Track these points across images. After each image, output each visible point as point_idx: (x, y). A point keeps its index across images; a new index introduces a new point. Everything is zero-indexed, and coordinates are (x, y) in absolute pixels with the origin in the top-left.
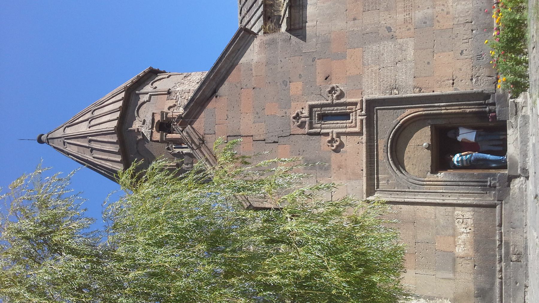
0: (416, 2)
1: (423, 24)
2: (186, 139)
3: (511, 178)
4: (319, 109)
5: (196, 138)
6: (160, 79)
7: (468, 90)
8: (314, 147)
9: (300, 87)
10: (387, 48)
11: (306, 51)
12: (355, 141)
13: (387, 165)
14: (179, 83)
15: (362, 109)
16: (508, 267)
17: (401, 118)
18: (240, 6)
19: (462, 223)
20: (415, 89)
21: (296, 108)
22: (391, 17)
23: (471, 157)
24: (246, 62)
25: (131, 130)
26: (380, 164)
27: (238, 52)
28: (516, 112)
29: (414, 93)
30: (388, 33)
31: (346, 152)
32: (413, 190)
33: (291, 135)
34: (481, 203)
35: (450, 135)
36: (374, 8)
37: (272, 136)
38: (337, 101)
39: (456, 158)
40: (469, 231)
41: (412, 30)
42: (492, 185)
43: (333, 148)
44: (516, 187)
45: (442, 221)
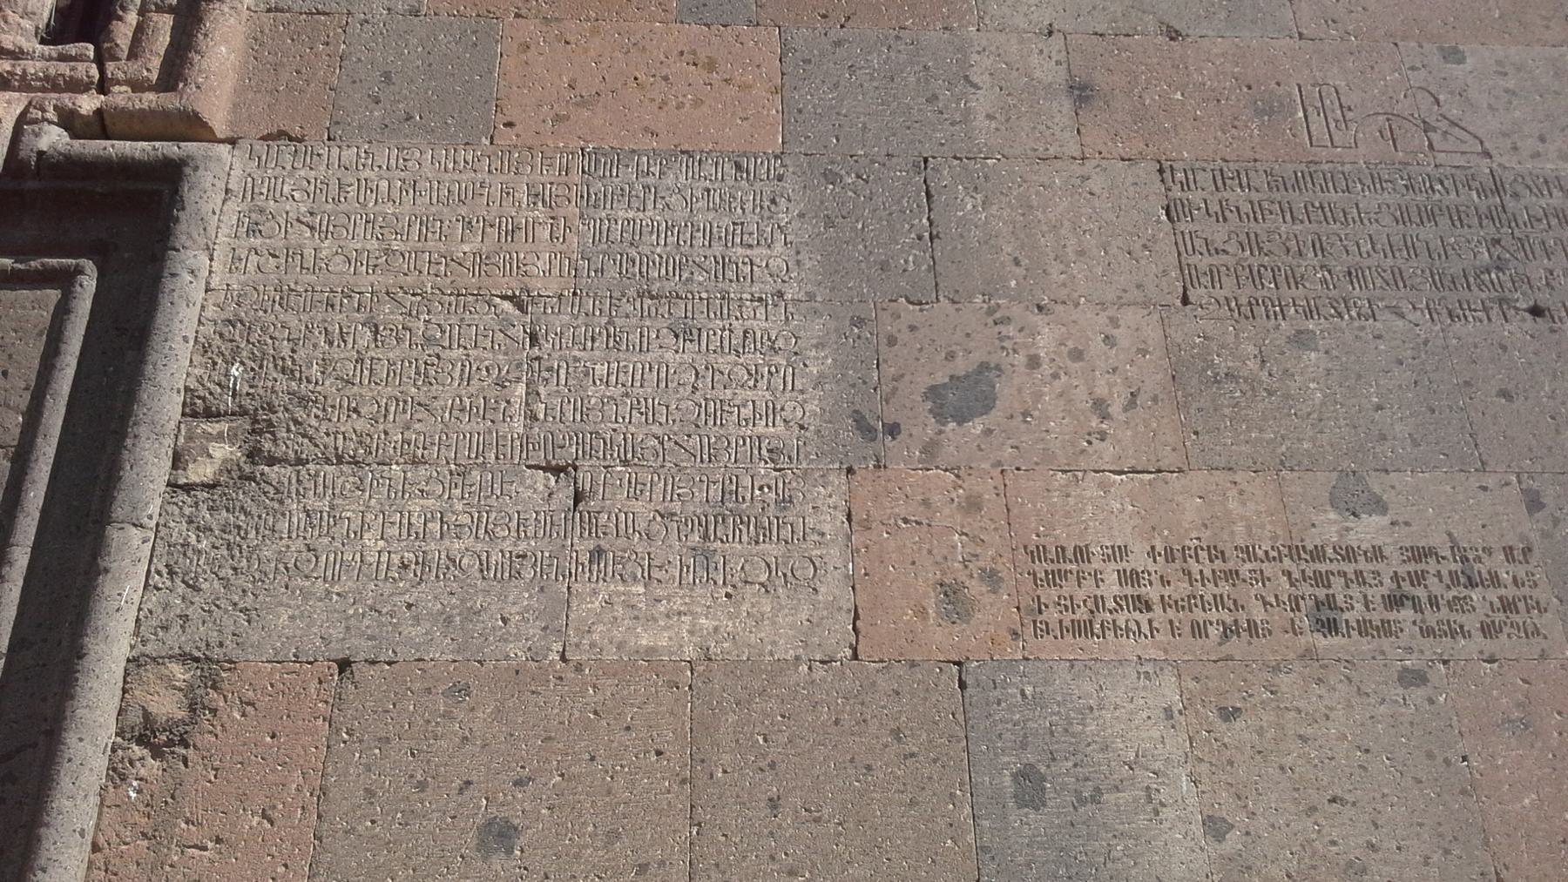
0: (1284, 680)
10: (755, 375)
20: (179, 672)
22: (1105, 417)
30: (924, 382)
36: (1203, 262)
41: (942, 638)
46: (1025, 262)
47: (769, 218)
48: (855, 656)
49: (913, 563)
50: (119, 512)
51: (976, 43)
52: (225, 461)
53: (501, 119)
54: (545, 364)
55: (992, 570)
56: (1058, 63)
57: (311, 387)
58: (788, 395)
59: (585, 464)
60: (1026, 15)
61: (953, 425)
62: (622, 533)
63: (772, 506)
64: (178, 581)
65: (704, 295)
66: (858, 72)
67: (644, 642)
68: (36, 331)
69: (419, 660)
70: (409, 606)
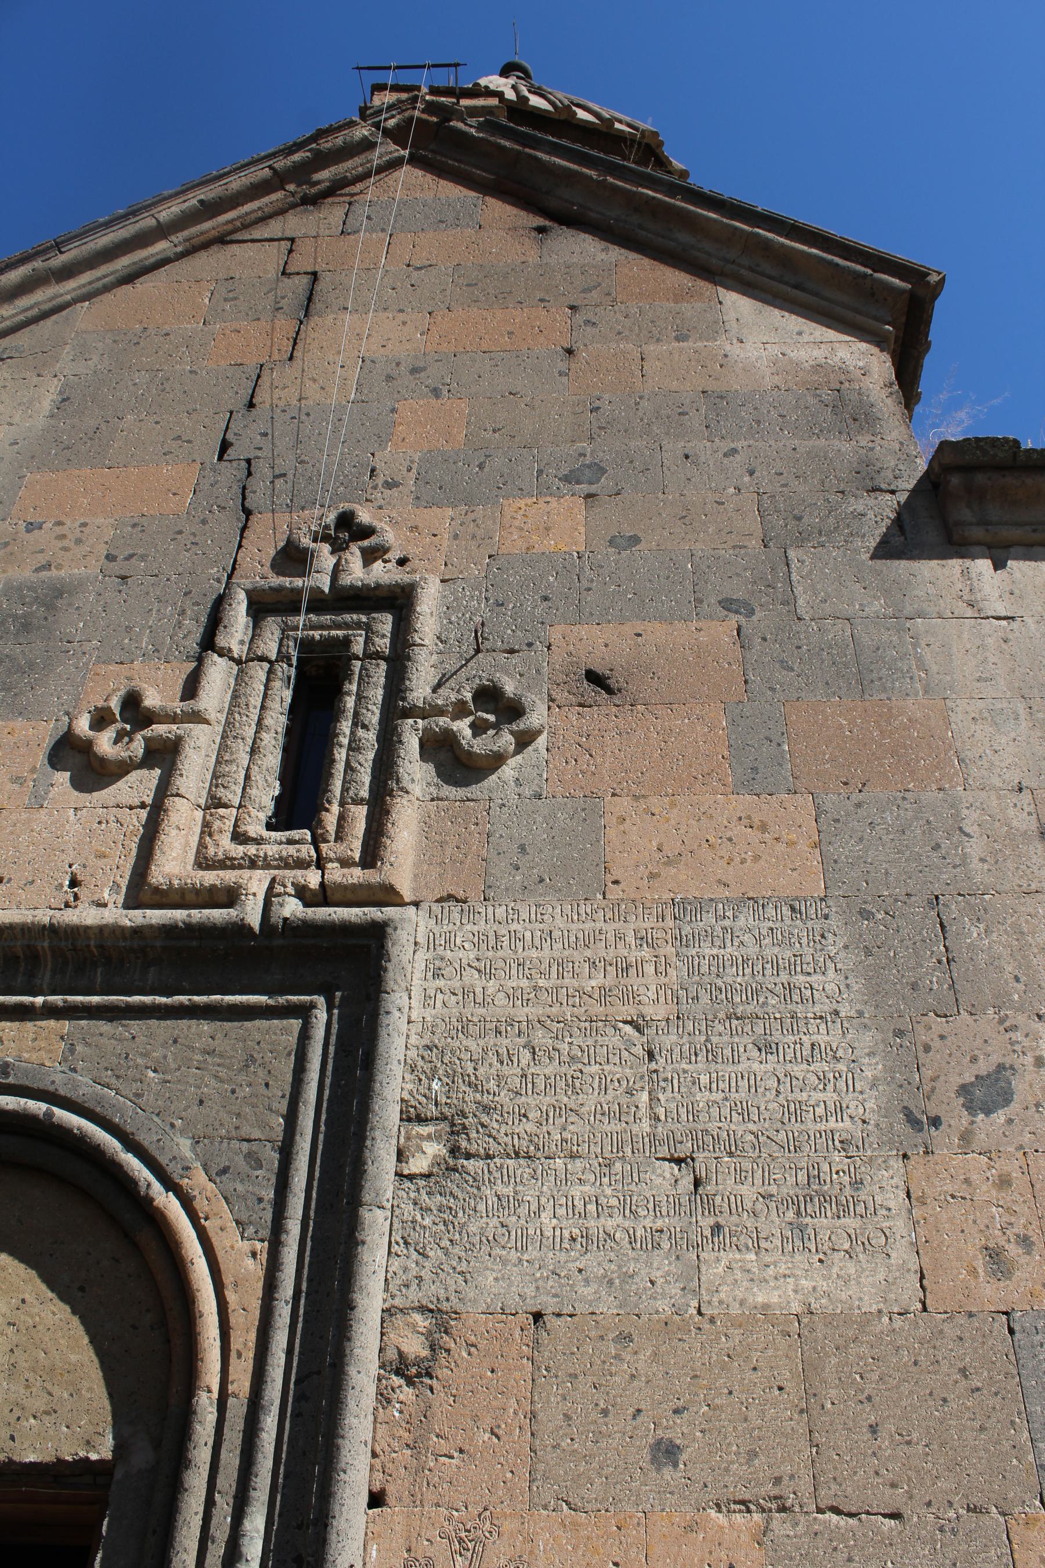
4: (383, 644)
8: (129, 629)
10: (822, 1079)
11: (794, 565)
12: (92, 861)
15: (323, 896)
17: (201, 1205)
21: (414, 528)
24: (730, 316)
27: (786, 283)
29: (388, 1312)
30: (956, 1081)
38: (411, 743)
46: (1023, 979)
47: (821, 950)
48: (925, 1309)
49: (963, 1231)
50: (367, 1197)
51: (964, 800)
52: (435, 1156)
53: (610, 878)
54: (662, 1076)
55: (1025, 1235)
56: (1030, 814)
57: (491, 1097)
58: (850, 1095)
59: (700, 1156)
60: (1000, 776)
61: (981, 1116)
62: (734, 1211)
63: (848, 1187)
64: (412, 1249)
65: (778, 1016)
66: (877, 828)
67: (760, 1299)
68: (286, 1052)
69: (593, 1313)
70: (580, 1271)
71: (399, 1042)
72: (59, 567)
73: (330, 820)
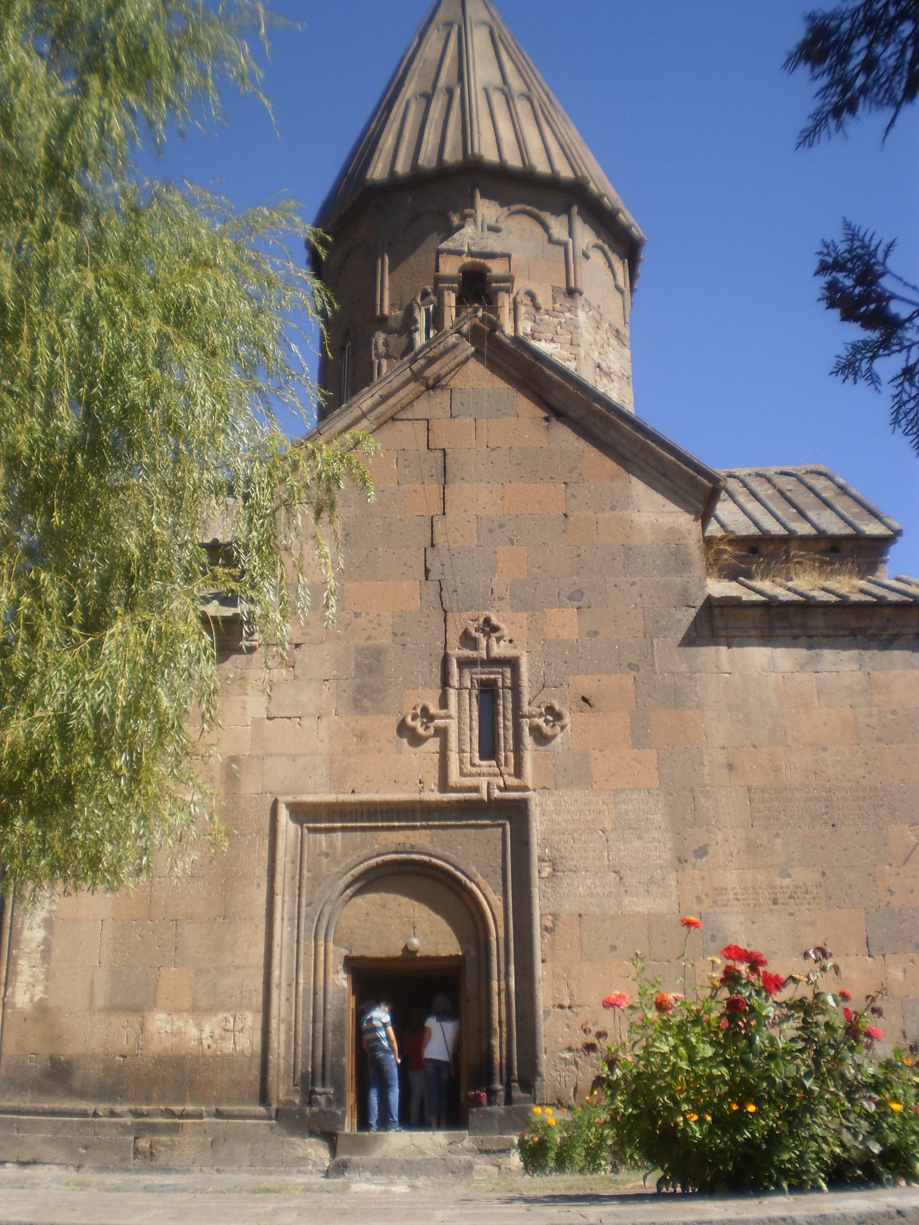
1: (710, 933)
2: (439, 343)
3: (330, 1138)
4: (508, 682)
5: (441, 368)
6: (611, 267)
7: (543, 1041)
8: (412, 672)
9: (565, 634)
10: (656, 848)
13: (365, 852)
14: (598, 317)
15: (506, 788)
16: (122, 1130)
17: (482, 886)
18: (800, 471)
19: (224, 1030)
20: (550, 917)
21: (513, 623)
23: (383, 1050)
25: (473, 197)
26: (368, 835)
28: (487, 1152)
29: (541, 916)
31: (399, 751)
32: (303, 914)
33: (445, 612)
34: (272, 1072)
35: (441, 1001)
36: (756, 815)
37: (443, 565)
38: (526, 729)
39: (381, 1015)
40: (205, 1043)
42: (314, 1096)
43: (409, 720)
44: (310, 1150)
45: (227, 981)
50: (533, 885)
59: (622, 871)
71: (535, 838)
72: (375, 638)
73: (502, 758)
